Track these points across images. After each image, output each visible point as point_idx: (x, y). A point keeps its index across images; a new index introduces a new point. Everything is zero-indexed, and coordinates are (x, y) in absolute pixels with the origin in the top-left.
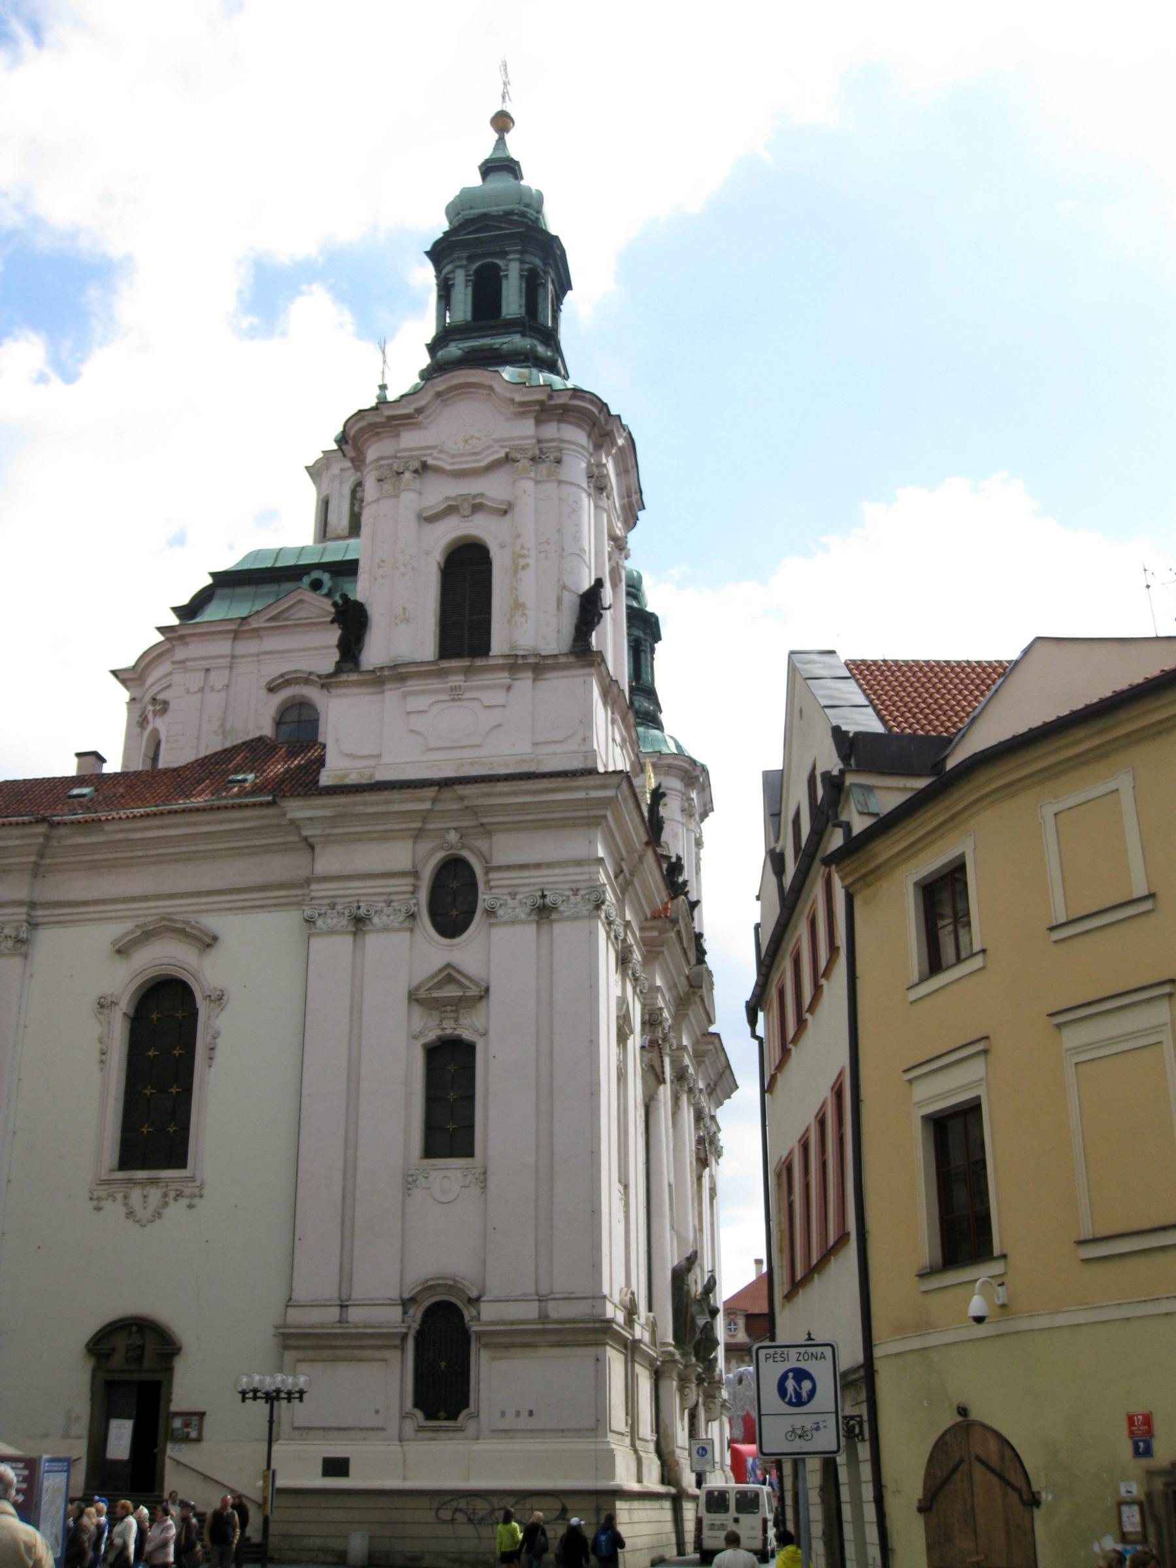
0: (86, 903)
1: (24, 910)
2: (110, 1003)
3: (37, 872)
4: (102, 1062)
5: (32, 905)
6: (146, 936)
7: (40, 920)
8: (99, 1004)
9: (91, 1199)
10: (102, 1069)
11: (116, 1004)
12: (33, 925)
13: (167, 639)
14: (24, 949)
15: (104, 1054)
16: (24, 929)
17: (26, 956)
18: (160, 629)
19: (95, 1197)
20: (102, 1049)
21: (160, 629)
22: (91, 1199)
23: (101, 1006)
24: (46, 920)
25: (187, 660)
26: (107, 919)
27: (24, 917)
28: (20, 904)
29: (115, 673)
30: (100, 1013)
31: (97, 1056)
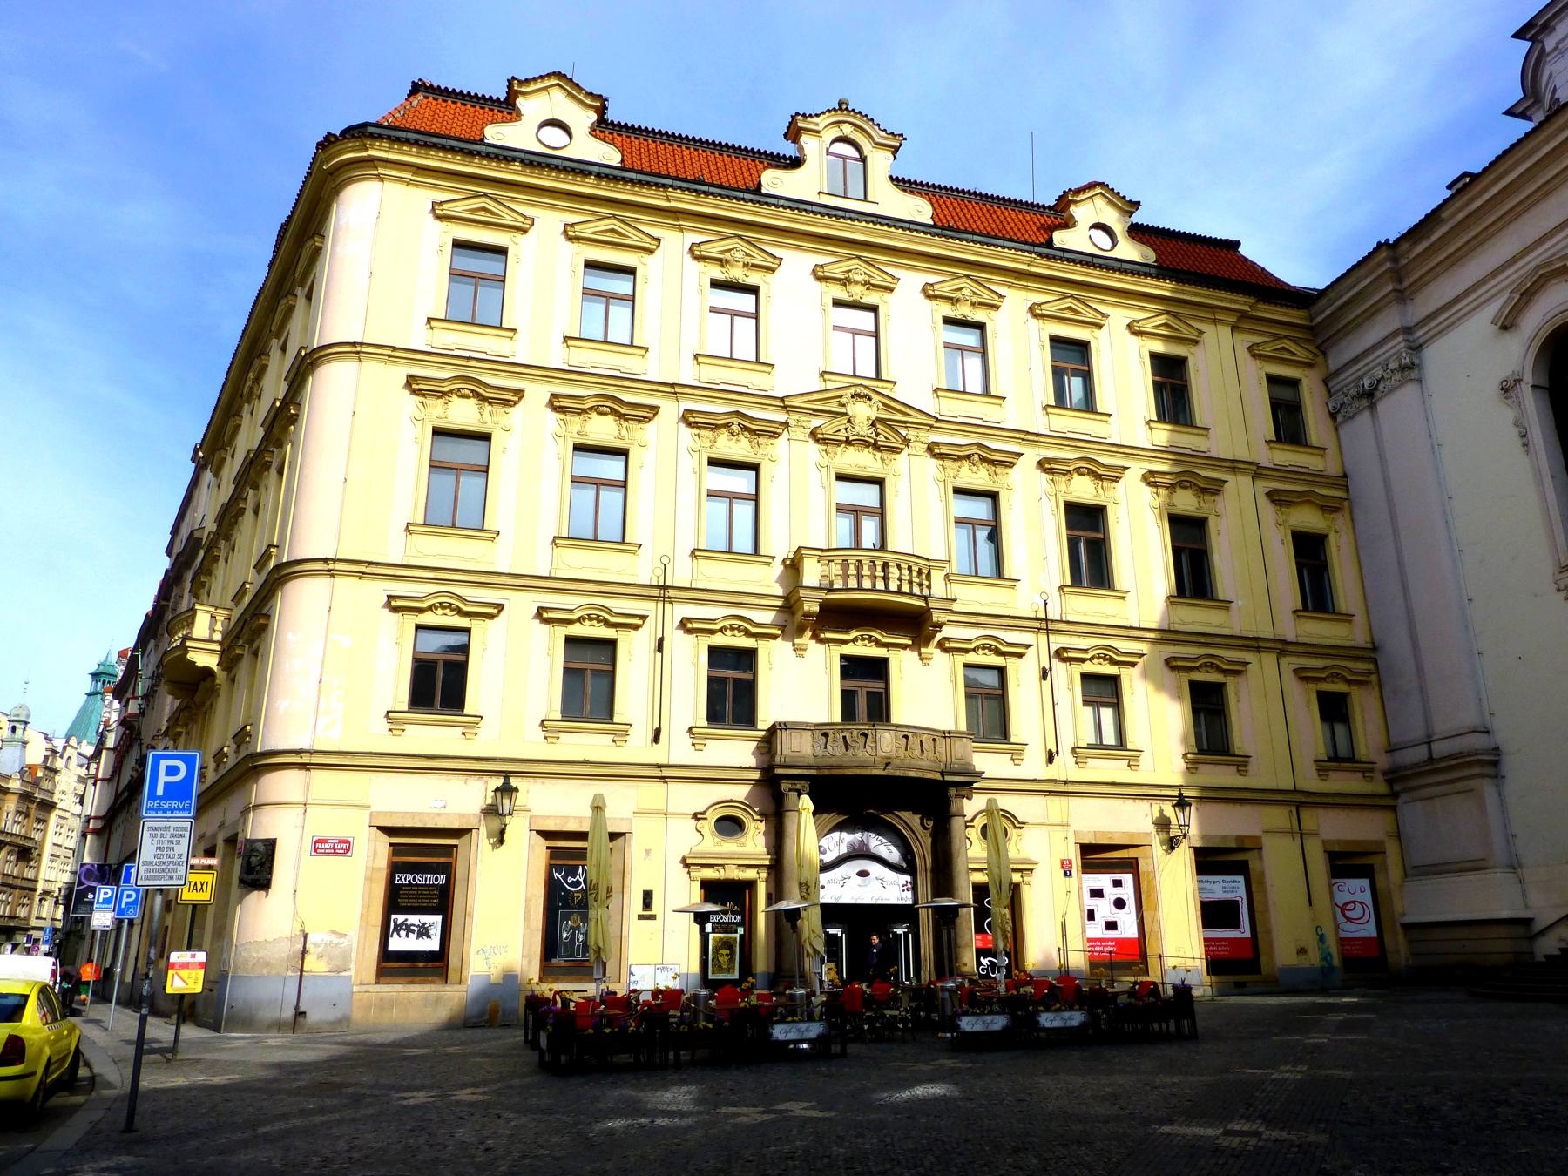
0: (1457, 300)
1: (1400, 338)
2: (1513, 383)
3: (1402, 296)
4: (1525, 445)
5: (1407, 330)
6: (1527, 296)
7: (1421, 341)
8: (1502, 389)
9: (1559, 590)
10: (1527, 452)
11: (1520, 380)
12: (1417, 348)
13: (1533, 39)
14: (1414, 374)
15: (1524, 436)
16: (1404, 355)
17: (1419, 381)
18: (1519, 35)
19: (1562, 587)
20: (1520, 432)
21: (1519, 35)
22: (1559, 590)
23: (1505, 390)
24: (1428, 336)
25: (1558, 43)
26: (1484, 302)
27: (1403, 345)
28: (1394, 334)
29: (1509, 112)
30: (1506, 398)
31: (1518, 442)
